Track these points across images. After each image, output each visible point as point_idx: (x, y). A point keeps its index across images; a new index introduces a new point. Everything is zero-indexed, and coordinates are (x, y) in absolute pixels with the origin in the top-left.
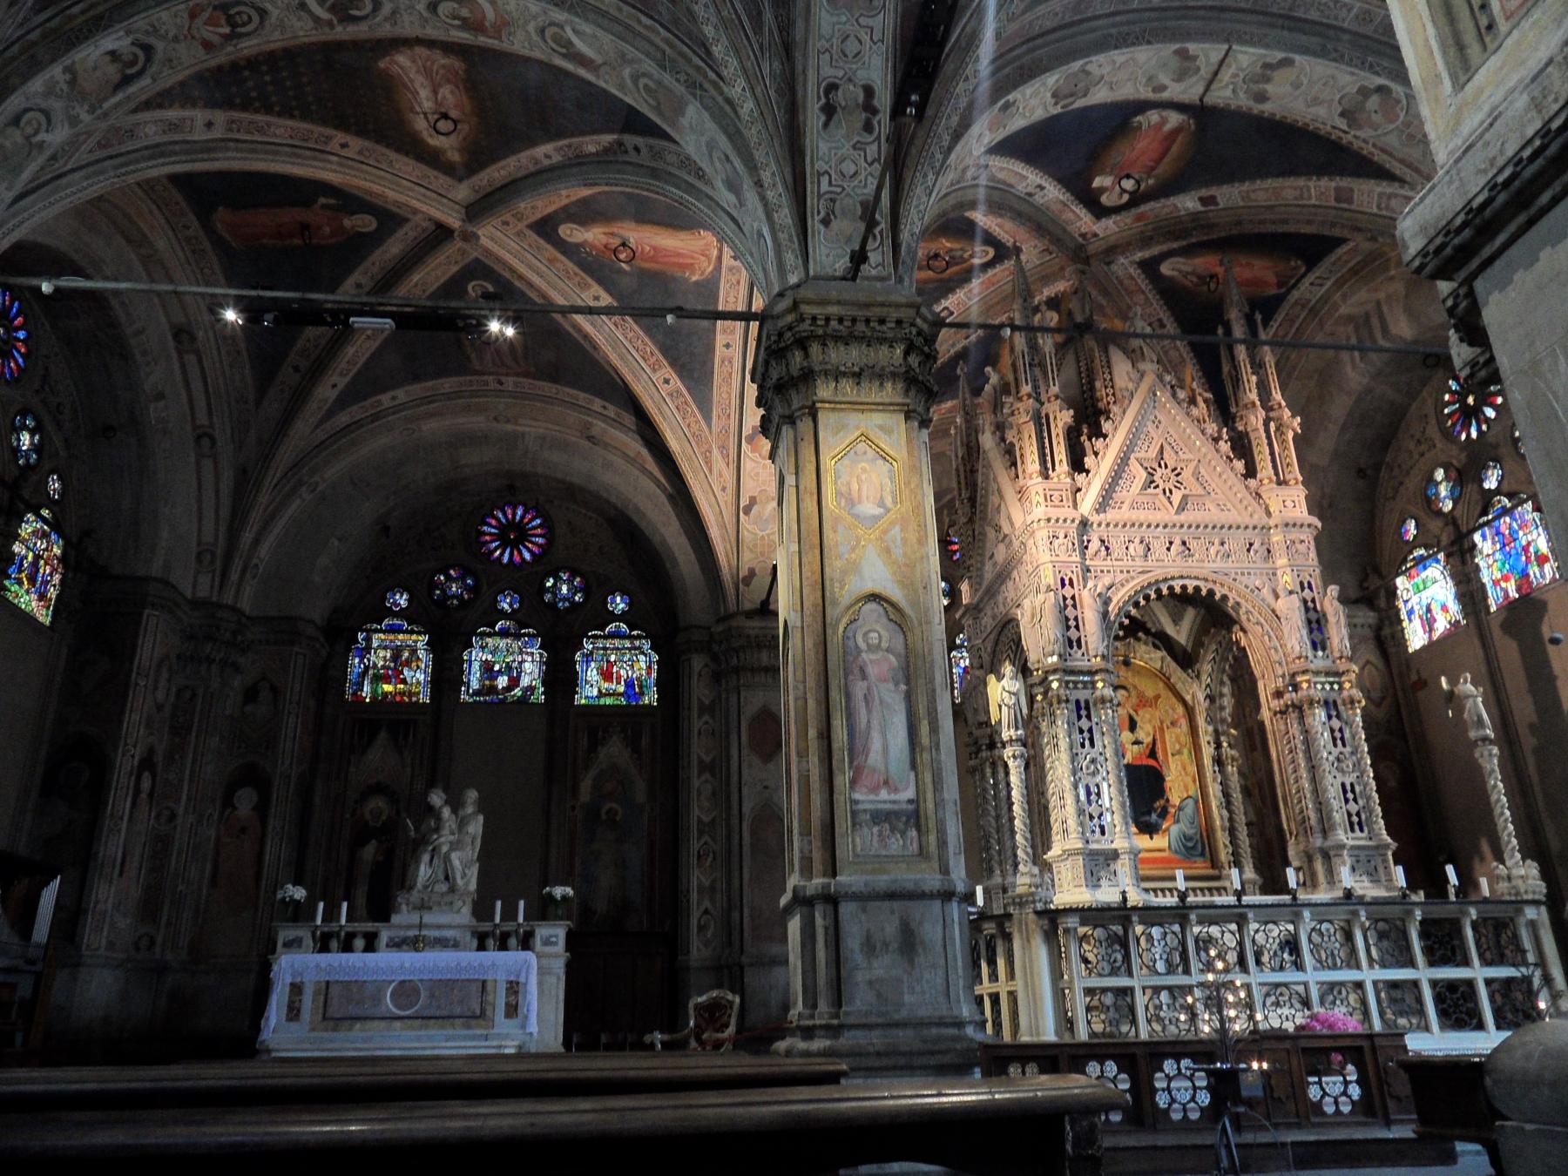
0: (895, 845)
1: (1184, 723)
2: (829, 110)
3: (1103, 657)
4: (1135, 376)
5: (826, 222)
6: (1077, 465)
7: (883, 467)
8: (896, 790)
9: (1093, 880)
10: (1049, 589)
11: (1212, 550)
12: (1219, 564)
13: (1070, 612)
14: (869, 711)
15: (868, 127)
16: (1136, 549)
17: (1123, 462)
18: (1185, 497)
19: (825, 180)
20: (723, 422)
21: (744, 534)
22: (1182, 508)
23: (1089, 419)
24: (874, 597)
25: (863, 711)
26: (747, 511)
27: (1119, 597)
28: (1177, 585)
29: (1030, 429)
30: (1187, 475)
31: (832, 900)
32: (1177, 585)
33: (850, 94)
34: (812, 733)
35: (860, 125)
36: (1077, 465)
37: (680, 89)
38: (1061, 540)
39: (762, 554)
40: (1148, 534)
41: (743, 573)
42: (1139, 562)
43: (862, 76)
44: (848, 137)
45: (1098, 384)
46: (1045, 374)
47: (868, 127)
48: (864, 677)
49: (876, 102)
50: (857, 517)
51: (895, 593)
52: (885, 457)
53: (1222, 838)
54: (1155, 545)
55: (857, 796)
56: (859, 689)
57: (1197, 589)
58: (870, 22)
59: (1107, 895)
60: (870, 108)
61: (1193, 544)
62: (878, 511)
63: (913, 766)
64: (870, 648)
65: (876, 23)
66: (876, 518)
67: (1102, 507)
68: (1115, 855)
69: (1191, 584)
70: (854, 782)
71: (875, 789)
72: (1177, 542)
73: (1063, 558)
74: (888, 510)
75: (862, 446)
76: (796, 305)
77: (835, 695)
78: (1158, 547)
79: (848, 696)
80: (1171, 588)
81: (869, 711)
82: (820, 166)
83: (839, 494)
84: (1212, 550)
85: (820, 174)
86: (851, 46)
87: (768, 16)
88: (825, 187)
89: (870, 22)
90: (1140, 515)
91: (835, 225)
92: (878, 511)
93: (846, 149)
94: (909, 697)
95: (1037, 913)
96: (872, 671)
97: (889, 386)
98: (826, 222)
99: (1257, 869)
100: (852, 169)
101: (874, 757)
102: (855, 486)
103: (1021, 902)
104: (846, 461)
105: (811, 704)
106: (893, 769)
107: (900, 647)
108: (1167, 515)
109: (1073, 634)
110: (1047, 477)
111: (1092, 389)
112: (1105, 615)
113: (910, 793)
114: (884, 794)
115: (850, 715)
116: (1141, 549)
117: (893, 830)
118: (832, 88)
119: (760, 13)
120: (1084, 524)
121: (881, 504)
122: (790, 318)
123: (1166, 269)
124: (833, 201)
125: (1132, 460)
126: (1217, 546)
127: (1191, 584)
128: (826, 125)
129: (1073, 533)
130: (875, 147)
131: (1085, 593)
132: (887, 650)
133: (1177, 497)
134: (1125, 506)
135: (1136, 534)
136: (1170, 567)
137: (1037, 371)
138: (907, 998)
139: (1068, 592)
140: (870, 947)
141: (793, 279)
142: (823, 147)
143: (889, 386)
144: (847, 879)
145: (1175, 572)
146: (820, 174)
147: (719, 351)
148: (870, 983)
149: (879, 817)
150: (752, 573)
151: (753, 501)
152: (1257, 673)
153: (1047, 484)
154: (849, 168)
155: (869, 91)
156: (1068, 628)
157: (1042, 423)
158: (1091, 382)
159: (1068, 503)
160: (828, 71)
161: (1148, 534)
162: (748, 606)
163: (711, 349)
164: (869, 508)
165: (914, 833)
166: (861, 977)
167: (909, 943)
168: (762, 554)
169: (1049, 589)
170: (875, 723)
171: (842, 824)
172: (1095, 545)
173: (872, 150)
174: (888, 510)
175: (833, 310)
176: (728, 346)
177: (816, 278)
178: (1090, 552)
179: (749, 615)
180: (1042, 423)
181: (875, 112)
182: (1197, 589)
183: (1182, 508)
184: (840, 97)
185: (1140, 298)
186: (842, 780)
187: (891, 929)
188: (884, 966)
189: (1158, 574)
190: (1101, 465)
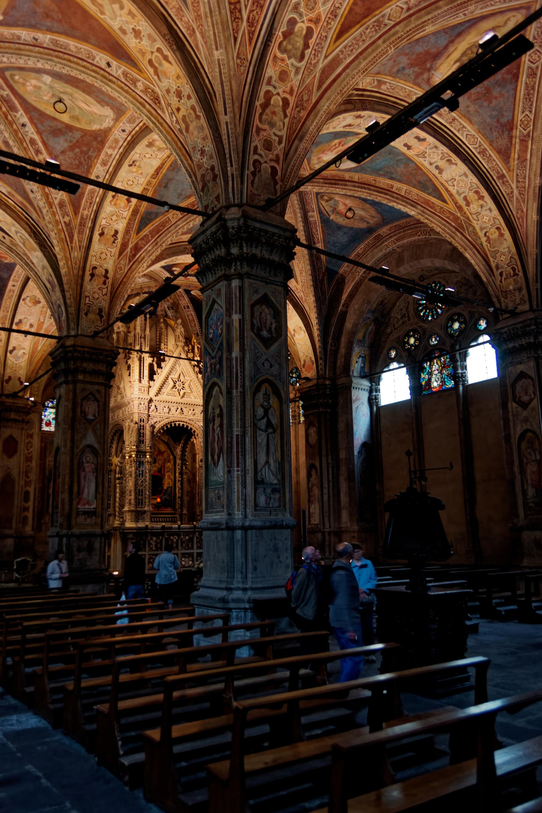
0: (89, 521)
1: (172, 461)
2: (92, 275)
3: (151, 448)
4: (175, 347)
5: (86, 314)
6: (151, 378)
7: (96, 404)
8: (90, 505)
9: (137, 520)
10: (136, 423)
11: (190, 412)
12: (192, 417)
13: (142, 431)
14: (85, 481)
15: (104, 283)
16: (166, 410)
17: (167, 378)
18: (184, 393)
19: (87, 299)
20: (5, 313)
21: (9, 362)
22: (183, 397)
23: (159, 357)
24: (90, 446)
25: (83, 481)
26: (11, 352)
27: (158, 426)
28: (177, 423)
29: (137, 363)
30: (186, 385)
31: (69, 537)
32: (177, 423)
33: (100, 271)
34: (66, 487)
35: (102, 282)
36: (151, 378)
37: (35, 246)
38: (142, 405)
39: (15, 371)
40: (170, 405)
41: (6, 378)
42: (167, 415)
43: (105, 266)
44: (97, 285)
45: (162, 344)
46: (145, 341)
47: (104, 283)
48: (84, 471)
49: (108, 275)
50: (87, 420)
51: (96, 446)
52: (96, 399)
53: (178, 501)
54: (172, 409)
55: (79, 507)
56: (82, 474)
57: (183, 425)
58: (111, 250)
59: (141, 525)
60: (106, 277)
61: (184, 410)
62: (93, 418)
63: (96, 498)
64: (88, 462)
65: (113, 250)
66: (93, 420)
67: (157, 395)
68: (145, 512)
69: (181, 423)
70: (78, 503)
71: (84, 505)
72: (180, 408)
73: (142, 412)
74: (96, 418)
75: (90, 396)
76: (74, 346)
77: (75, 477)
78: (173, 409)
79: (79, 477)
80: (175, 424)
81: (85, 481)
82: (87, 294)
83: (81, 411)
84: (190, 412)
85: (86, 297)
86: (103, 256)
87: (76, 237)
88: (87, 301)
89: (111, 250)
90: (170, 398)
91: (89, 316)
92: (93, 418)
93: (96, 289)
94: (96, 478)
95: (120, 532)
96: (87, 469)
97: (101, 377)
98: (86, 314)
99: (188, 511)
100: (97, 296)
101: (85, 495)
102: (87, 409)
103: (115, 529)
104: (85, 401)
105: (67, 478)
106: (90, 498)
107: (95, 462)
108: (178, 399)
109: (141, 438)
110: (140, 381)
111: (160, 345)
112: (152, 432)
113: (94, 506)
114: (87, 506)
115: (79, 482)
116: (167, 410)
117: (88, 517)
118: (95, 268)
119: (73, 236)
120: (151, 401)
121: (94, 416)
122: (71, 349)
123: (192, 292)
124: (89, 307)
125: (169, 378)
126: (192, 411)
127: (181, 423)
128: (91, 280)
129: (146, 404)
130: (106, 290)
131: (147, 425)
132: (92, 463)
133: (182, 392)
134: (165, 394)
135: (167, 405)
136: (175, 416)
137: (143, 340)
138: (88, 564)
139: (142, 423)
140: (79, 550)
141: (73, 333)
142: (89, 287)
143: (101, 377)
144: (76, 531)
145: (177, 419)
146: (86, 297)
147: (10, 286)
148: (79, 560)
149: (85, 513)
150: (10, 378)
151: (14, 348)
152: (197, 452)
153: (141, 385)
154: (96, 296)
155: (107, 271)
156: (140, 436)
157: (141, 360)
158: (160, 342)
159: (146, 392)
160: (94, 263)
161: (170, 405)
162: (6, 392)
163: (5, 286)
164: (90, 417)
165: (94, 518)
166: (76, 558)
167: (90, 549)
168: (15, 371)
169: (136, 423)
170: (86, 485)
171: (74, 515)
172: (153, 408)
173: (105, 291)
174: (96, 418)
175: (86, 349)
176: (14, 286)
177: (81, 335)
178: (151, 410)
179: (8, 396)
180: (141, 360)
181: (107, 278)
182: (183, 425)
183: (183, 397)
184: (97, 272)
185: (182, 298)
186: (75, 502)
187: (85, 543)
188: (82, 555)
189: (172, 419)
190: (159, 378)
